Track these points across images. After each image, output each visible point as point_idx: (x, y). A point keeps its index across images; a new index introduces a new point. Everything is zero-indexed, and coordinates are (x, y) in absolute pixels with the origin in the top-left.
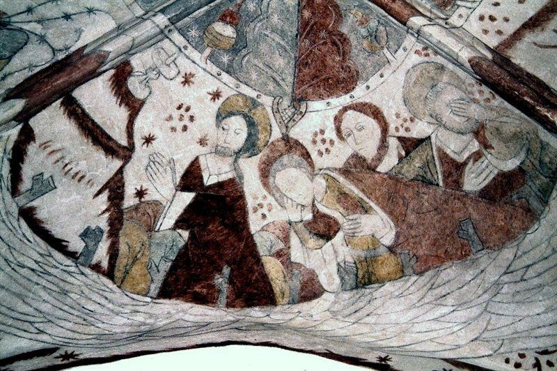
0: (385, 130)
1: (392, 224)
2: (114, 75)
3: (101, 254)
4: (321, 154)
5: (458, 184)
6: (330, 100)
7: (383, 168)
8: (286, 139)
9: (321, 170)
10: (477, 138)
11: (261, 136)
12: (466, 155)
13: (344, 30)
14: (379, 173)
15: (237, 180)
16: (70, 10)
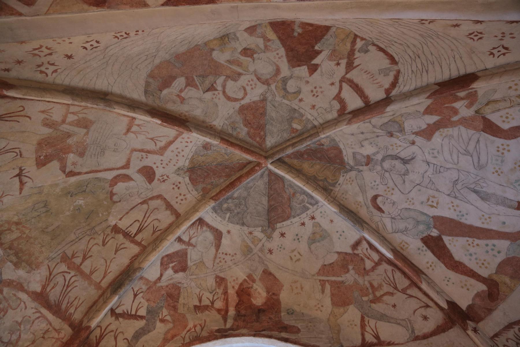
0: (224, 92)
1: (214, 58)
2: (345, 111)
3: (359, 44)
4: (252, 80)
5: (187, 78)
6: (250, 101)
7: (222, 78)
8: (269, 84)
9: (252, 74)
10: (183, 98)
11: (280, 85)
12: (186, 90)
13: (246, 129)
14: (224, 76)
15: (291, 68)
16: (361, 135)
